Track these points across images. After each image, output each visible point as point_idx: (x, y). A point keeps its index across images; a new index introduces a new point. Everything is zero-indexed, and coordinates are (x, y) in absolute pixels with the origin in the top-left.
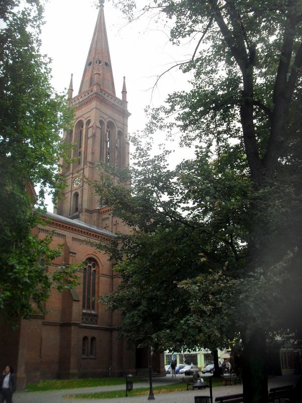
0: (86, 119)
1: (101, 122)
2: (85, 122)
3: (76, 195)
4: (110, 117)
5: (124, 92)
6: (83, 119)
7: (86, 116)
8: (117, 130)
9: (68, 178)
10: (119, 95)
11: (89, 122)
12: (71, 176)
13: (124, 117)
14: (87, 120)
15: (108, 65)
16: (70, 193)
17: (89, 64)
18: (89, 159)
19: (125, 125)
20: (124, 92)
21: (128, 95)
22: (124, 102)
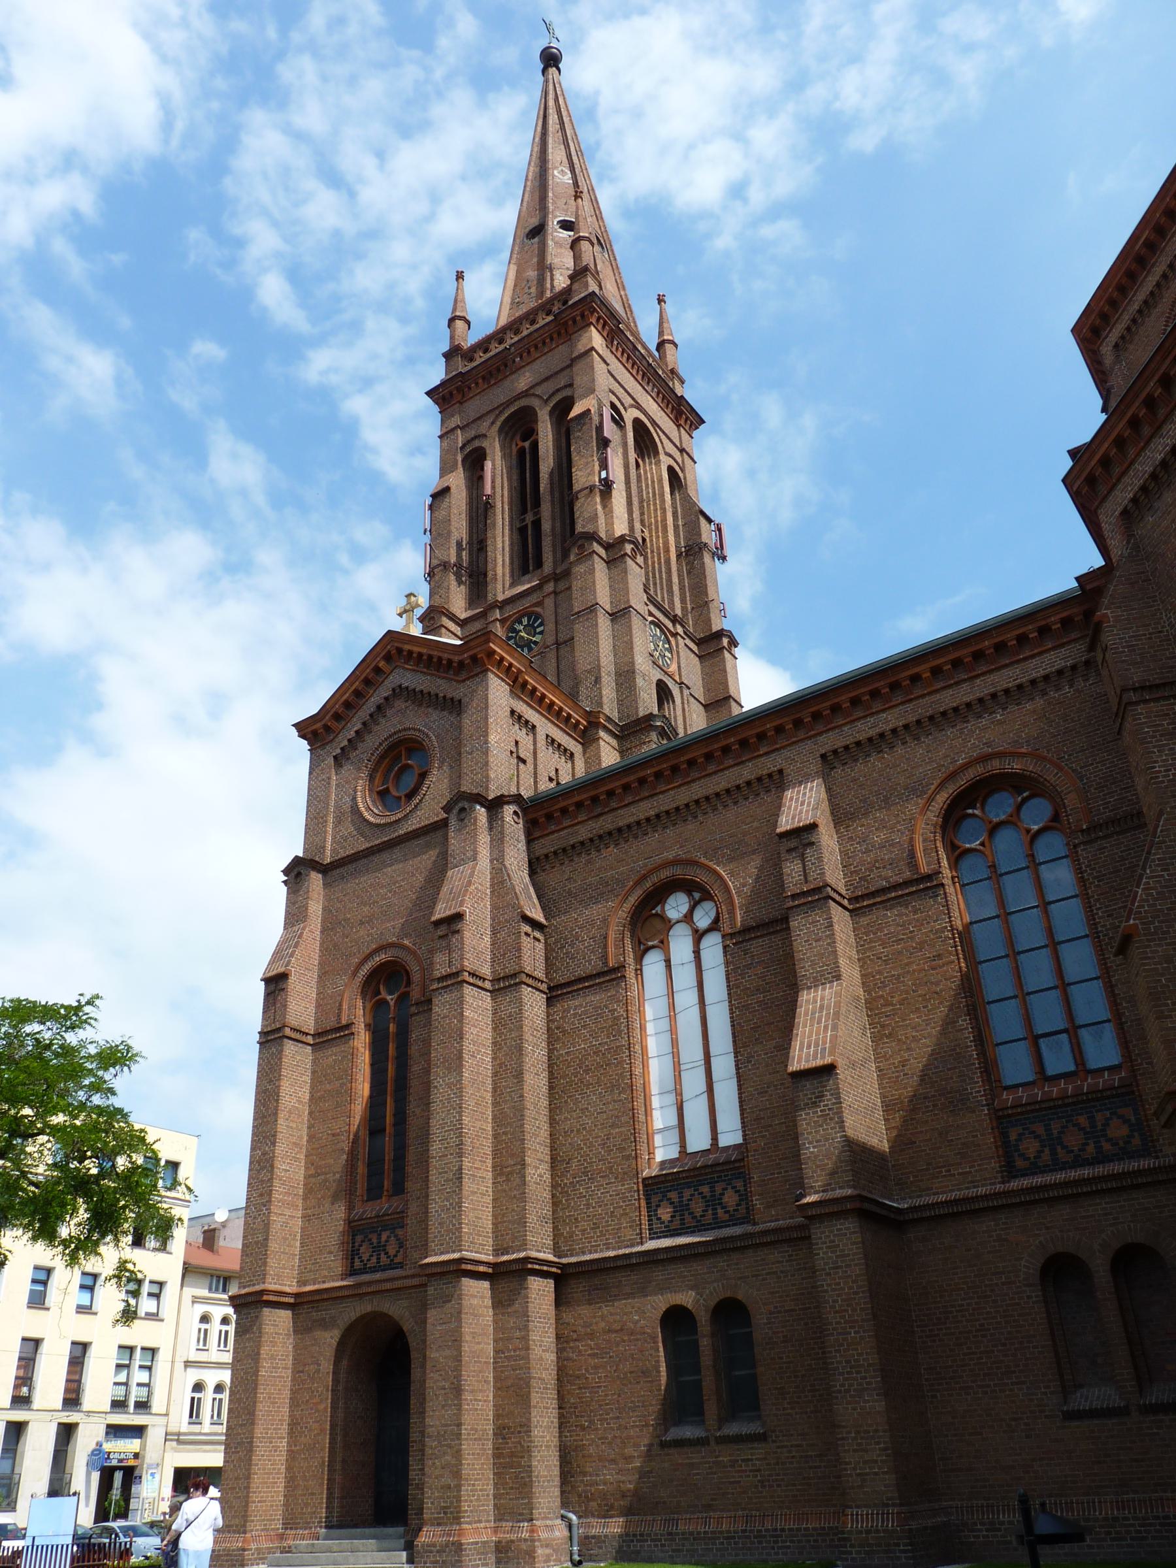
6: (535, 403)
13: (678, 426)
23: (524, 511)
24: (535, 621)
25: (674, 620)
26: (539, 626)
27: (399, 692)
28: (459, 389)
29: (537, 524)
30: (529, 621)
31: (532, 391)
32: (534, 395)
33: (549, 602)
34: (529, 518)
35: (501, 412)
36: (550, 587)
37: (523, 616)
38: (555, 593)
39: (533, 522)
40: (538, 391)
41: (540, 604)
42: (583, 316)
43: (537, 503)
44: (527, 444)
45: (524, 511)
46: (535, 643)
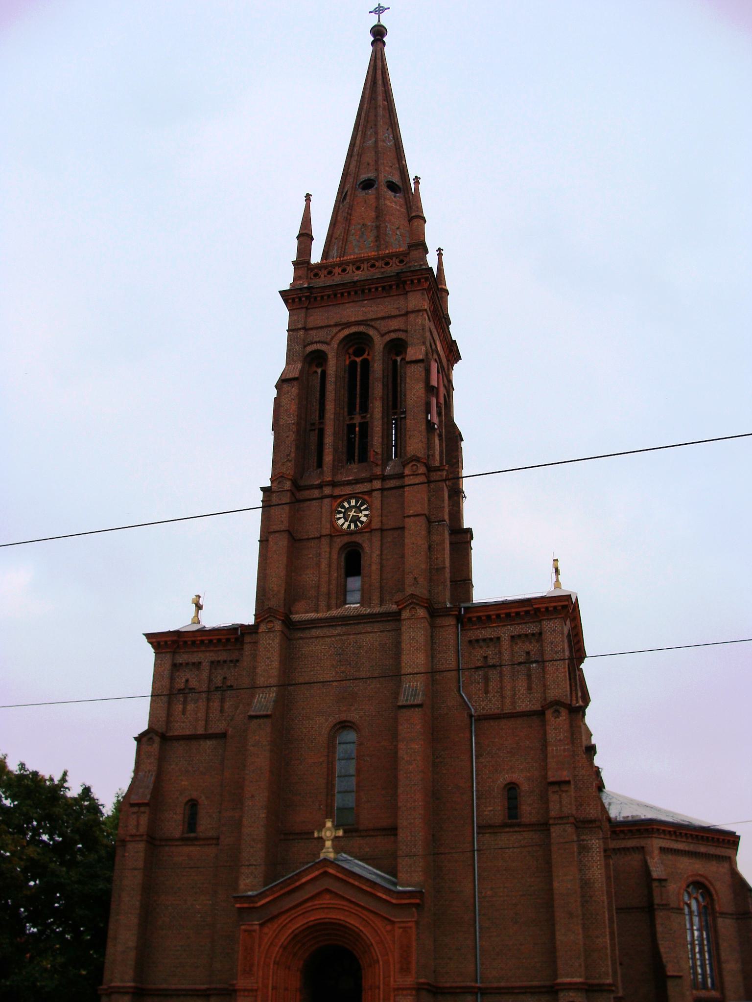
0: (382, 335)
2: (379, 343)
6: (371, 332)
7: (383, 326)
9: (316, 493)
11: (397, 347)
14: (387, 338)
16: (325, 542)
24: (362, 505)
26: (365, 510)
28: (307, 298)
29: (365, 427)
30: (356, 503)
31: (373, 323)
32: (372, 326)
34: (357, 420)
35: (343, 329)
36: (377, 484)
37: (352, 498)
38: (382, 490)
39: (361, 424)
40: (377, 324)
41: (370, 493)
42: (419, 280)
43: (365, 408)
44: (358, 360)
46: (362, 522)
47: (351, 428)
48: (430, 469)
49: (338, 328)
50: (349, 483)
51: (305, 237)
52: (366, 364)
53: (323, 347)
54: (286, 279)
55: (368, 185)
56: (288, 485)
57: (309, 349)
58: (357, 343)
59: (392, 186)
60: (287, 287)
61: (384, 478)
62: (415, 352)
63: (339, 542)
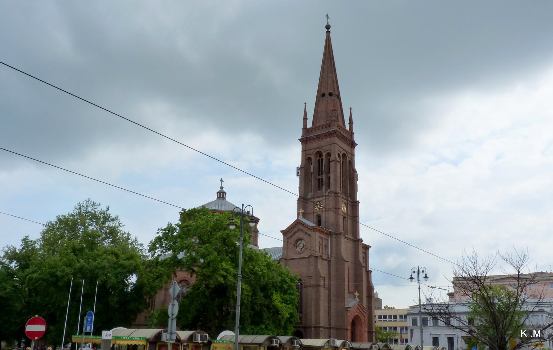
0: (325, 151)
1: (339, 155)
2: (324, 154)
3: (319, 217)
4: (344, 150)
5: (351, 123)
6: (323, 151)
8: (348, 159)
10: (347, 127)
11: (329, 155)
12: (312, 200)
14: (327, 152)
15: (338, 97)
17: (321, 95)
18: (332, 188)
19: (353, 155)
20: (351, 123)
21: (354, 125)
22: (351, 133)
23: (319, 175)
25: (348, 200)
27: (300, 229)
33: (324, 201)
36: (324, 198)
40: (324, 148)
41: (322, 200)
45: (319, 175)
47: (319, 179)
48: (336, 193)
49: (313, 150)
50: (318, 197)
51: (305, 119)
52: (322, 159)
53: (310, 156)
54: (300, 134)
55: (323, 95)
56: (302, 200)
57: (307, 157)
58: (319, 154)
59: (331, 95)
60: (301, 138)
61: (326, 196)
62: (332, 158)
63: (315, 214)
